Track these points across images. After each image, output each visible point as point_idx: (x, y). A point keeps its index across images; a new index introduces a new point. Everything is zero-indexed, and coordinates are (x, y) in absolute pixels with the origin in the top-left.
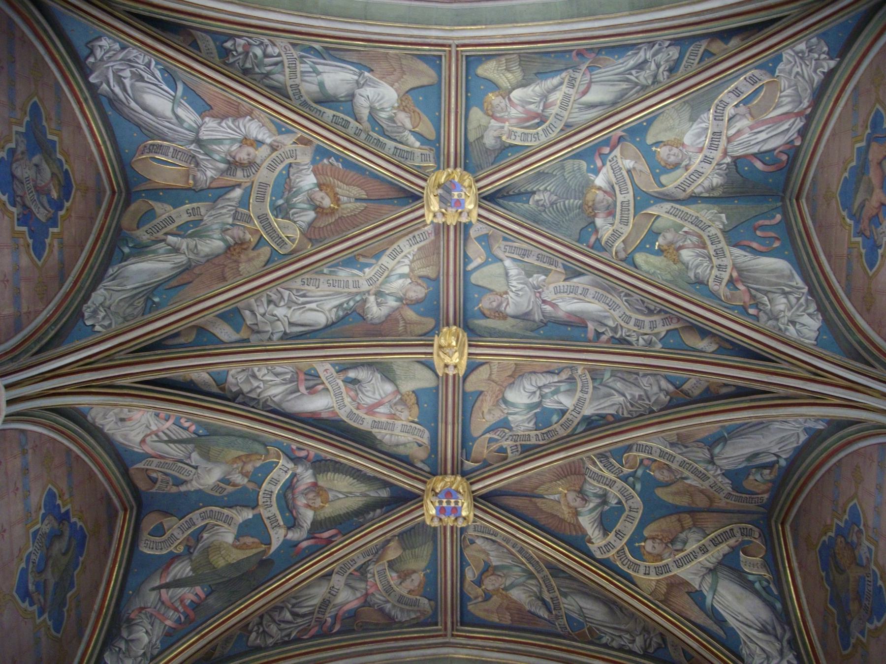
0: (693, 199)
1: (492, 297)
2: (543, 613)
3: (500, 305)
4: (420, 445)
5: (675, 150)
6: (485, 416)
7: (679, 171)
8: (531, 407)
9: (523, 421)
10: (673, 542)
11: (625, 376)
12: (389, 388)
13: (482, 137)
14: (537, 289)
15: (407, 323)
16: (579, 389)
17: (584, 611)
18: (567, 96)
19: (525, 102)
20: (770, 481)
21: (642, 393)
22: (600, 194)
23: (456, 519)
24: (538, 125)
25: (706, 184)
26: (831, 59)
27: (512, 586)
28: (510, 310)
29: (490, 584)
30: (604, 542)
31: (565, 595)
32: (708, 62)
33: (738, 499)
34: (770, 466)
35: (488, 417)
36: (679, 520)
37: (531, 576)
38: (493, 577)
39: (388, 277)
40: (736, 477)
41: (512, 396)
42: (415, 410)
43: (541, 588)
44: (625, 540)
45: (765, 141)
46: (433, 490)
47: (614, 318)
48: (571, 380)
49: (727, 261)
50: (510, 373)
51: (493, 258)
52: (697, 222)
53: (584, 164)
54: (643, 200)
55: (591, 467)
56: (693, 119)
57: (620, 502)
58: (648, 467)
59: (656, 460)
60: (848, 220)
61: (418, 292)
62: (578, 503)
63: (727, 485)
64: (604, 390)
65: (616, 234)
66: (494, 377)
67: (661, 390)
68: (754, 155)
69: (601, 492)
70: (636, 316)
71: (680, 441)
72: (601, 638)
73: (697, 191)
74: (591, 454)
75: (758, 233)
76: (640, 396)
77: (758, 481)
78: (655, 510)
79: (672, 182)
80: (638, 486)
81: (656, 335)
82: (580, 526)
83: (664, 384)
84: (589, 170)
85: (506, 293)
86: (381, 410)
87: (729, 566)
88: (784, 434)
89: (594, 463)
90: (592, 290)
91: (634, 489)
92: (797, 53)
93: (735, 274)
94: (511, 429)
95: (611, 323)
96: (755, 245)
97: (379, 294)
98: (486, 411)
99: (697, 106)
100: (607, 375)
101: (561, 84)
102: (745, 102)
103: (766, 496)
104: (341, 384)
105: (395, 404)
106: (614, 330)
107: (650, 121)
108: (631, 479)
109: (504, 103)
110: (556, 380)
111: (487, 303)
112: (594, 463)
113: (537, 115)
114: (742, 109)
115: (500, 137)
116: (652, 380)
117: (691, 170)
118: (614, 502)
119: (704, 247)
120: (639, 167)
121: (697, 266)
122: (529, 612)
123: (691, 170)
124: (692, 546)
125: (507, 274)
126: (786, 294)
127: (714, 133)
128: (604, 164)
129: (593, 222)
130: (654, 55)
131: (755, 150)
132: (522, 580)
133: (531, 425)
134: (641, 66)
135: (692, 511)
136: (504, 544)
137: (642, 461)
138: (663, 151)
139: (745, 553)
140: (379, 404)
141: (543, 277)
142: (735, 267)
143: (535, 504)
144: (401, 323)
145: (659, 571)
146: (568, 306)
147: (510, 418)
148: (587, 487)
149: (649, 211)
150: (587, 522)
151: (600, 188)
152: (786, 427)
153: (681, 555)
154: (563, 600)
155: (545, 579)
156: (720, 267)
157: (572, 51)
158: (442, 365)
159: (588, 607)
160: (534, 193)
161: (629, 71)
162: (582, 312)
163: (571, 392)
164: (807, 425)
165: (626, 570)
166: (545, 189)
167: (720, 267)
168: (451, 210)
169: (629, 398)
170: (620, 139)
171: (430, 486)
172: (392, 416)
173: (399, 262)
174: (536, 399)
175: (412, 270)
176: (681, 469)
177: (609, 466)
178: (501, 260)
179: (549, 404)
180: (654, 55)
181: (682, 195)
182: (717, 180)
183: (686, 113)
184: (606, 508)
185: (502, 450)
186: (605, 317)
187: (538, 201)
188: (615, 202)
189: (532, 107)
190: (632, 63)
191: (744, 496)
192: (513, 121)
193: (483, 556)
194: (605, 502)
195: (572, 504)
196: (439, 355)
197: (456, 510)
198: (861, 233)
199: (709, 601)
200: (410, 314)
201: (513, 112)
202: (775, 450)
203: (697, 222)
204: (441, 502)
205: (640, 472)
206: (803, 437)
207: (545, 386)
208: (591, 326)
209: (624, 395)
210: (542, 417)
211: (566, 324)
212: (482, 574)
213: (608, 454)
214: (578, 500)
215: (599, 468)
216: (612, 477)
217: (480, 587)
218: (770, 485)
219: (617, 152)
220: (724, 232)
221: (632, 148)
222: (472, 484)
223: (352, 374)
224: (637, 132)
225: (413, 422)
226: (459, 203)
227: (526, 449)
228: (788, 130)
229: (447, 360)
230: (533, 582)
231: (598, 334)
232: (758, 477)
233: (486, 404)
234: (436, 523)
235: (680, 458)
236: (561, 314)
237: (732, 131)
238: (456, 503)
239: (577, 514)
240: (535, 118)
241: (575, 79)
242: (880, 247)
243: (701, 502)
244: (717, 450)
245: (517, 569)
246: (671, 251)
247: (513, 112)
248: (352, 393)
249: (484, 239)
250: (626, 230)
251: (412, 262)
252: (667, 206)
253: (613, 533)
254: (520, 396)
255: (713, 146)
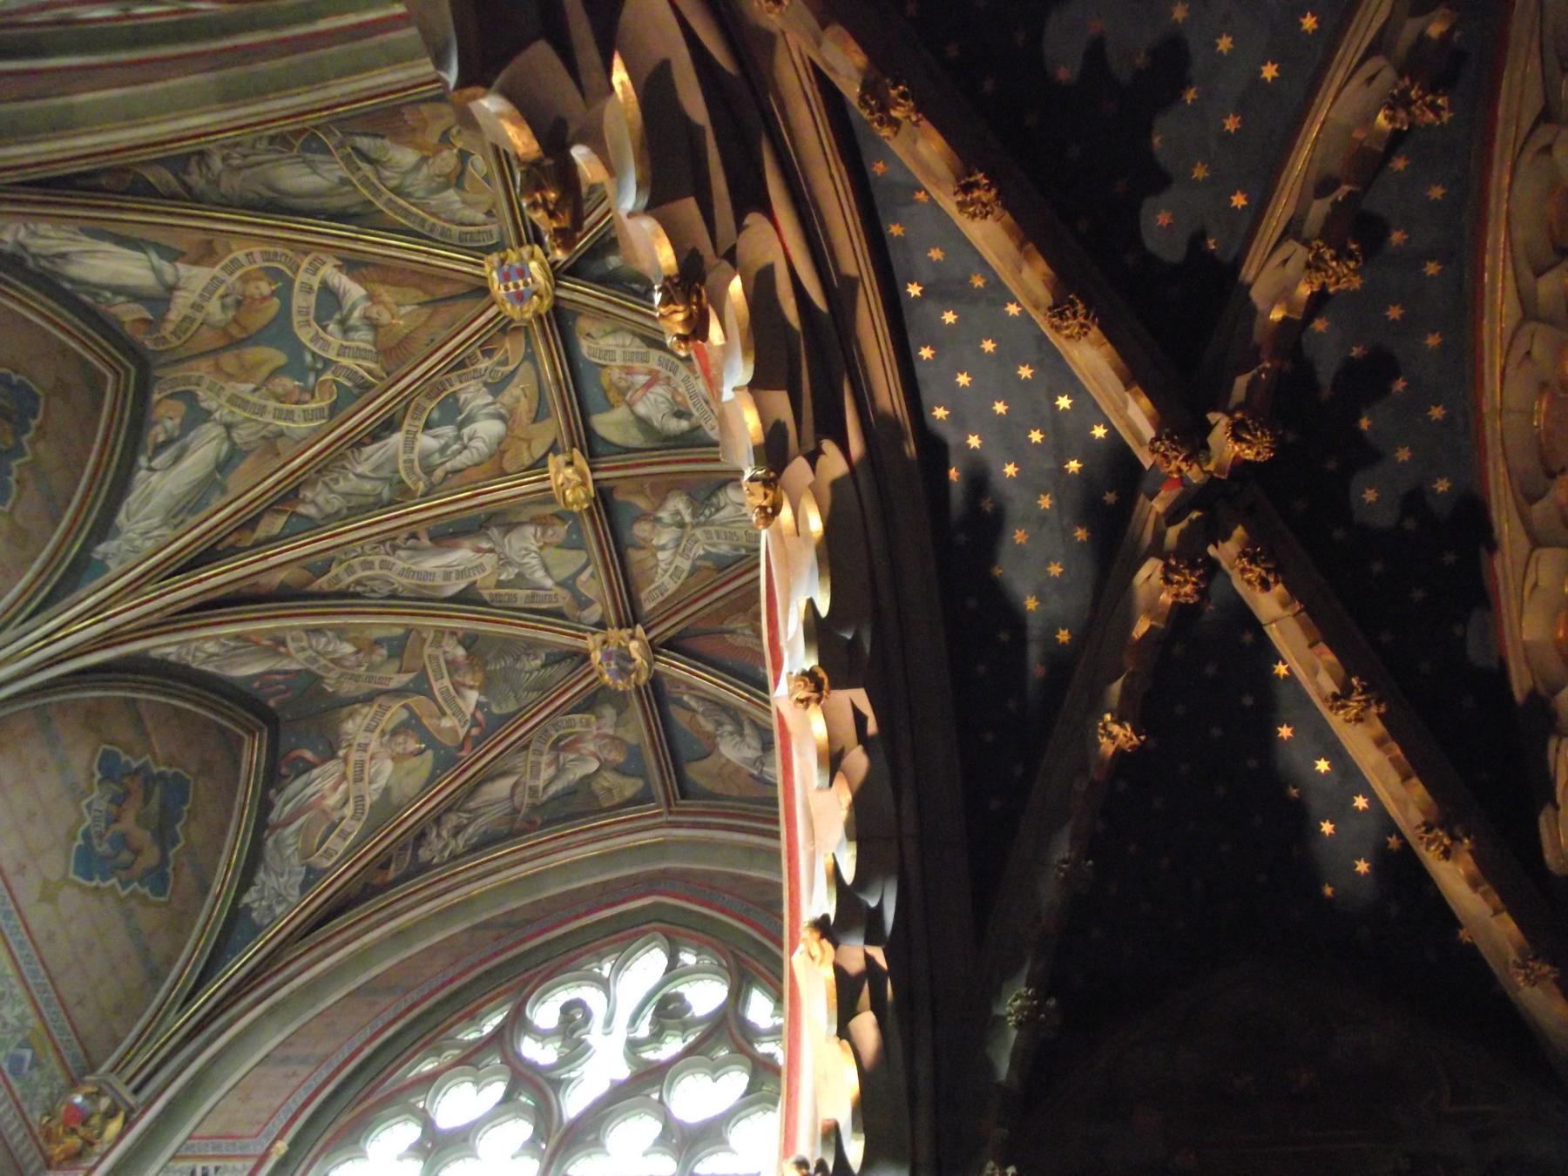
0: (368, 699)
1: (555, 540)
2: (364, 143)
3: (543, 534)
4: (589, 335)
5: (399, 749)
6: (519, 394)
7: (390, 726)
8: (470, 419)
9: (474, 398)
10: (239, 303)
11: (363, 500)
12: (641, 409)
13: (619, 714)
14: (505, 562)
15: (640, 492)
16: (416, 463)
17: (308, 170)
18: (536, 775)
19: (581, 759)
20: (156, 423)
21: (335, 487)
22: (469, 680)
23: (503, 261)
24: (559, 739)
25: (359, 719)
26: (247, 906)
27: (417, 167)
28: (529, 530)
29: (448, 159)
30: (321, 273)
31: (344, 182)
32: (382, 859)
33: (187, 381)
34: (160, 448)
35: (518, 392)
36: (244, 329)
37: (397, 191)
38: (448, 170)
39: (678, 546)
40: (197, 416)
41: (496, 427)
42: (605, 382)
43: (380, 178)
44: (297, 285)
45: (307, 785)
46: (541, 297)
47: (401, 561)
48: (429, 470)
49: (301, 656)
50: (507, 456)
51: (568, 584)
52: (356, 678)
53: (496, 710)
54: (421, 686)
55: (372, 365)
56: (387, 790)
57: (324, 328)
58: (303, 390)
59: (297, 403)
60: (163, 769)
61: (641, 530)
62: (374, 313)
63: (207, 401)
64: (385, 473)
65: (437, 643)
66: (525, 446)
67: (313, 502)
68: (315, 766)
69: (352, 334)
70: (377, 572)
71: (272, 442)
72: (271, 143)
73: (365, 710)
74: (380, 385)
75: (282, 687)
76: (336, 481)
77: (167, 417)
78: (279, 331)
79: (395, 713)
80: (308, 358)
81: (341, 562)
82: (359, 282)
83: (310, 510)
84: (487, 705)
85: (541, 548)
86: (642, 379)
87: (158, 300)
88: (147, 509)
89: (370, 372)
90: (439, 581)
91: (314, 354)
92: (285, 900)
93: (282, 649)
94: (486, 384)
95: (402, 553)
96: (278, 677)
97: (681, 525)
98: (523, 399)
99: (387, 808)
100: (386, 494)
101: (545, 788)
102: (333, 826)
103: (156, 397)
104: (694, 411)
105: (629, 388)
106: (395, 548)
107: (432, 779)
108: (319, 365)
109: (605, 754)
110: (448, 465)
111: (561, 530)
112: (370, 372)
113: (564, 749)
114: (336, 816)
115: (598, 718)
116: (329, 509)
117: (378, 731)
118: (332, 327)
119: (332, 660)
120: (435, 721)
121: (329, 642)
122: (383, 137)
123: (378, 731)
124: (214, 307)
125: (547, 569)
126: (212, 655)
127: (362, 780)
128: (473, 715)
129: (467, 648)
130: (445, 847)
131: (316, 772)
132: (408, 181)
133: (462, 397)
134: (457, 831)
135: (235, 344)
136: (447, 225)
137: (313, 396)
138: (413, 745)
139: (144, 321)
140: (648, 386)
141: (503, 577)
142: (288, 655)
143: (426, 292)
144: (648, 491)
145: (236, 264)
146: (462, 555)
147: (490, 399)
148: (370, 336)
149: (411, 676)
150: (354, 291)
151: (471, 688)
152: (142, 524)
153: (221, 290)
154: (346, 173)
155: (377, 192)
156: (303, 649)
157: (543, 826)
158: (576, 462)
159: (305, 179)
160: (544, 666)
161: (471, 821)
162: (443, 553)
163: (425, 456)
164: (116, 543)
165: (279, 250)
166: (531, 673)
167: (303, 649)
168: (613, 648)
169: (351, 476)
170: (462, 747)
171: (547, 302)
172: (629, 371)
173: (671, 564)
174: (466, 431)
175: (654, 555)
176: (263, 402)
177: (351, 375)
178: (558, 584)
179: (448, 431)
180: (445, 847)
181: (381, 700)
182: (349, 726)
183: (396, 796)
184: (337, 316)
185: (488, 353)
186: (410, 558)
187: (536, 658)
188: (451, 676)
189: (571, 757)
190: (470, 830)
191: (182, 388)
192: (589, 737)
193: (469, 197)
194: (342, 322)
195: (381, 308)
196: (581, 474)
197: (506, 277)
198: (137, 772)
199: (155, 258)
200: (642, 504)
201: (591, 747)
202: (155, 478)
203: (356, 678)
204: (526, 284)
205: (311, 379)
206: (121, 518)
207: (459, 452)
208: (425, 542)
209: (357, 475)
210: (453, 412)
211: (455, 535)
212: (462, 173)
213: (356, 391)
214: (375, 315)
215: (363, 367)
216: (345, 361)
217: (460, 151)
218: (154, 417)
219: (462, 732)
220: (321, 678)
221: (447, 740)
222: (499, 313)
223: (684, 424)
224: (447, 760)
225: (604, 366)
226: (607, 656)
227: (461, 365)
228: (285, 804)
229: (569, 471)
230: (393, 183)
231: (414, 536)
232: (169, 424)
233: (524, 408)
234: (526, 250)
235: (268, 418)
236: (467, 543)
237: (342, 787)
238: (507, 288)
239: (371, 297)
240: (566, 745)
241: (530, 796)
242: (100, 782)
243: (229, 361)
244: (225, 447)
245: (421, 194)
246: (367, 647)
247: (591, 747)
248: (679, 399)
249: (583, 603)
250: (427, 650)
251: (656, 566)
252: (393, 685)
253: (316, 287)
254: (487, 430)
255: (361, 765)
